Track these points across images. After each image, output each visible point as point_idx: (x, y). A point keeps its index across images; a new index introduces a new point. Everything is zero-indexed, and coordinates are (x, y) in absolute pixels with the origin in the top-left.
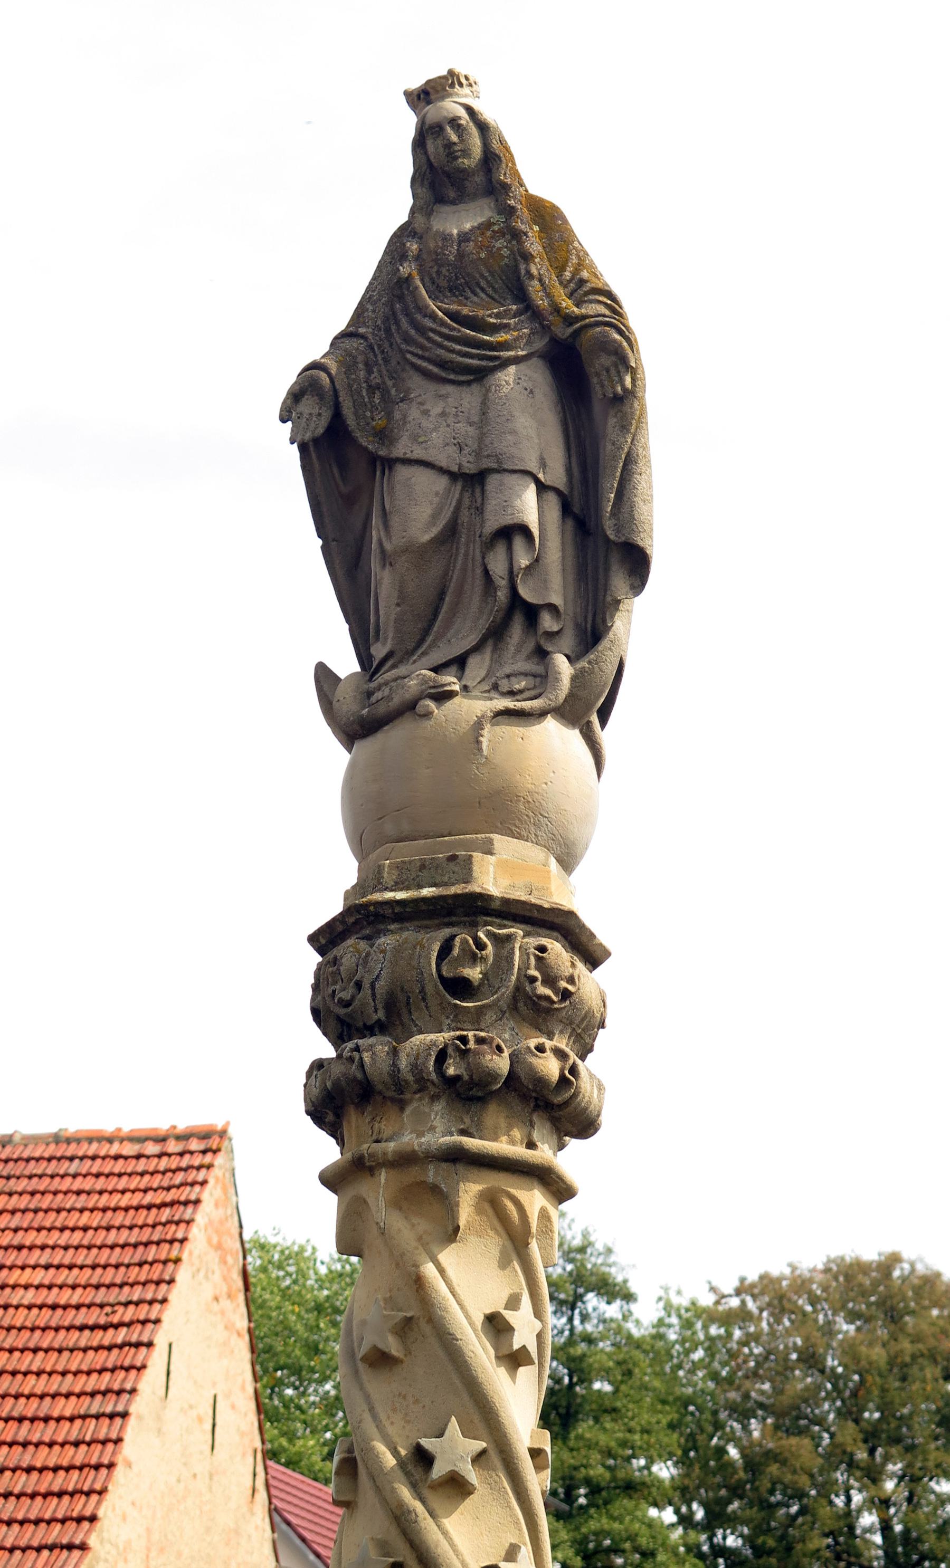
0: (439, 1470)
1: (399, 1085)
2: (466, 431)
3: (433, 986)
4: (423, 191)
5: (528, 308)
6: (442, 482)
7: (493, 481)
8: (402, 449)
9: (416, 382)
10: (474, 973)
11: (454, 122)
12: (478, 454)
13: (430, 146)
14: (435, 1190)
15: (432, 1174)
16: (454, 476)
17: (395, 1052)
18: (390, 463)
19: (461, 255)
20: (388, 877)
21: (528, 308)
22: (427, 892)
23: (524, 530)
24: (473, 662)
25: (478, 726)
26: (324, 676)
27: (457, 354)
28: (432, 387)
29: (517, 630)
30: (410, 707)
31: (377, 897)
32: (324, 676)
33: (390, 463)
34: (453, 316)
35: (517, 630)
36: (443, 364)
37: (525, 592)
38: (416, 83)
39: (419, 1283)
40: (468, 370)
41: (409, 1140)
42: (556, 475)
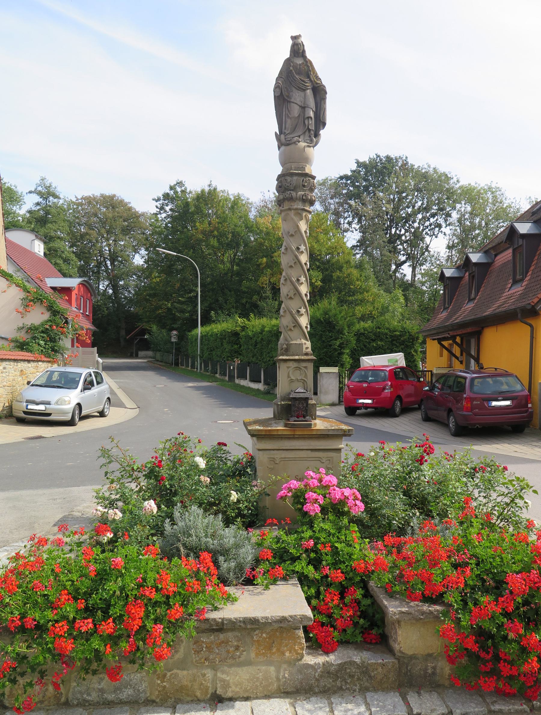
0: (301, 250)
1: (296, 199)
2: (302, 99)
3: (301, 185)
4: (292, 54)
5: (310, 80)
6: (298, 107)
7: (307, 109)
8: (292, 100)
9: (294, 89)
10: (306, 184)
11: (300, 44)
12: (304, 104)
13: (295, 47)
14: (300, 214)
15: (299, 211)
16: (300, 106)
17: (297, 194)
18: (290, 102)
19: (300, 68)
20: (293, 168)
21: (310, 80)
22: (300, 172)
23: (311, 118)
24: (301, 136)
25: (304, 147)
26: (276, 133)
27: (301, 86)
28: (297, 91)
29: (307, 133)
30: (295, 143)
31: (292, 171)
32: (276, 133)
33: (290, 102)
34: (300, 79)
35: (307, 133)
36: (298, 87)
37: (310, 127)
38: (294, 35)
39: (298, 226)
40: (303, 89)
41: (295, 207)
42: (314, 109)
